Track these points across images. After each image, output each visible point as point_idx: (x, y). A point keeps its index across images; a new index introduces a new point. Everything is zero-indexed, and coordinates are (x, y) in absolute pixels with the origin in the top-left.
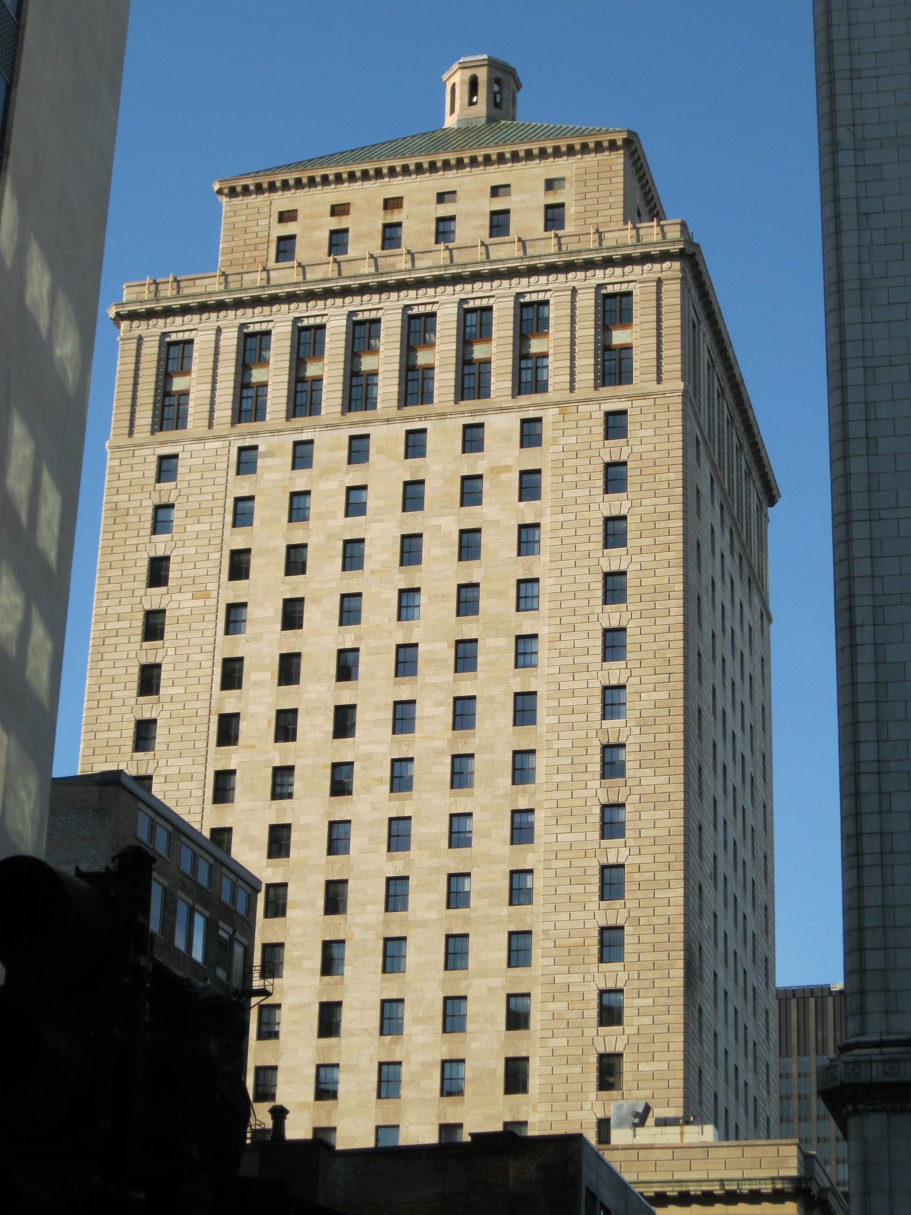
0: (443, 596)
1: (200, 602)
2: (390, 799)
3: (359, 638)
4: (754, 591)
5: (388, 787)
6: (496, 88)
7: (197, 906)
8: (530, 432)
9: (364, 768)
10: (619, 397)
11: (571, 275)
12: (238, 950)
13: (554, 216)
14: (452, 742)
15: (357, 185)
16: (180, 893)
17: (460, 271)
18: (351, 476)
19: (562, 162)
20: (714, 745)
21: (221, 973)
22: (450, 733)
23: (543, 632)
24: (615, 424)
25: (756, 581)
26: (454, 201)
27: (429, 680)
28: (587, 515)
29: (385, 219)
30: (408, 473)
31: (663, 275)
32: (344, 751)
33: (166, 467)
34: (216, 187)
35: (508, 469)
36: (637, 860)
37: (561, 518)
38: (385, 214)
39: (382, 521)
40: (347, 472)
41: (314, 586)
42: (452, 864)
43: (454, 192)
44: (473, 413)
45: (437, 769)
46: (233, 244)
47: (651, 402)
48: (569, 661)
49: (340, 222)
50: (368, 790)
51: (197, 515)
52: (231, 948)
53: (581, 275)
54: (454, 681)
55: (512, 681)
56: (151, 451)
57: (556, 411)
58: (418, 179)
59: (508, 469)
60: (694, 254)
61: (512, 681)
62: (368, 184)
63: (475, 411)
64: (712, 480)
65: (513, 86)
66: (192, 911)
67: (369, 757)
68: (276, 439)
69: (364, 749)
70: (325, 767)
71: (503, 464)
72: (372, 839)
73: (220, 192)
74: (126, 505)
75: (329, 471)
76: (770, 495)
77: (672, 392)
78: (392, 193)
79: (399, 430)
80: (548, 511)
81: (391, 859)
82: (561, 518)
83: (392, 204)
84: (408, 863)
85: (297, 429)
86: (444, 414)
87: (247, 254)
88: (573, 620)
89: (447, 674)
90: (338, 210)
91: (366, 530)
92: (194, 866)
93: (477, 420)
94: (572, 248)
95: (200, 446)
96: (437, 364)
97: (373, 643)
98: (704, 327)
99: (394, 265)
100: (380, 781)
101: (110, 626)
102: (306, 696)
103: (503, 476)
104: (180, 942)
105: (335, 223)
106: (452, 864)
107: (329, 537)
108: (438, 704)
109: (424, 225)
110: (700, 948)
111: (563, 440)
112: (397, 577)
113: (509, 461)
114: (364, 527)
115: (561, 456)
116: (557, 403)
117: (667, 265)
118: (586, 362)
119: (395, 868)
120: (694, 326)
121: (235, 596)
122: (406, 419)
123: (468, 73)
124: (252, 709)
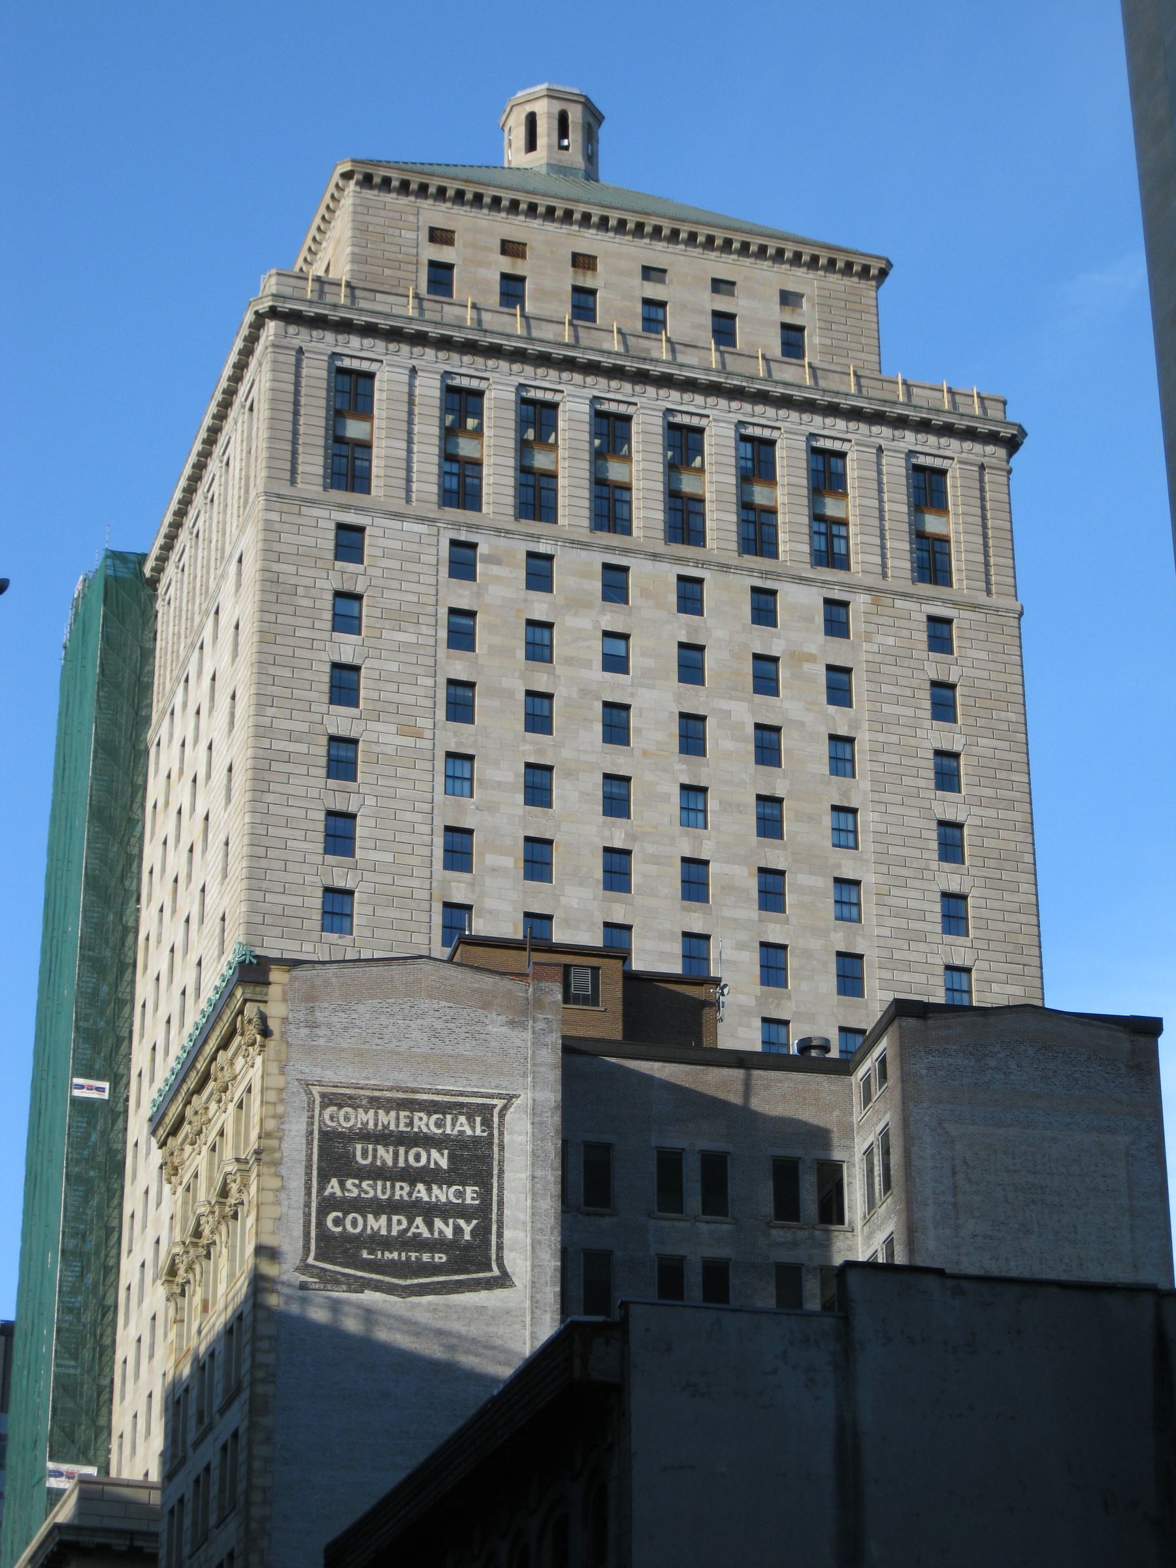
0: (739, 805)
1: (409, 741)
3: (633, 837)
8: (836, 619)
10: (944, 601)
11: (876, 429)
13: (792, 340)
15: (551, 227)
17: (744, 384)
18: (608, 617)
19: (799, 274)
22: (758, 989)
23: (869, 879)
24: (939, 634)
26: (663, 282)
27: (727, 913)
28: (912, 741)
29: (575, 279)
30: (684, 632)
31: (986, 461)
33: (349, 543)
34: (347, 167)
35: (811, 658)
37: (881, 737)
38: (575, 273)
39: (653, 687)
40: (602, 612)
41: (566, 753)
43: (664, 271)
44: (765, 574)
46: (367, 252)
47: (981, 617)
48: (903, 923)
49: (514, 265)
51: (399, 618)
54: (760, 921)
55: (833, 936)
56: (325, 514)
58: (617, 240)
59: (811, 658)
61: (833, 936)
63: (767, 573)
68: (502, 542)
71: (805, 650)
73: (347, 176)
74: (293, 580)
75: (576, 603)
77: (1008, 611)
79: (669, 573)
80: (866, 725)
82: (881, 737)
85: (532, 536)
86: (728, 567)
87: (387, 272)
88: (904, 872)
89: (752, 911)
91: (632, 695)
93: (768, 584)
94: (834, 387)
95: (396, 524)
96: (708, 496)
97: (651, 849)
99: (648, 350)
101: (277, 745)
102: (564, 900)
103: (807, 666)
105: (507, 265)
107: (584, 692)
108: (741, 946)
109: (628, 304)
111: (879, 639)
112: (679, 767)
113: (812, 648)
114: (630, 690)
115: (878, 658)
117: (990, 449)
118: (900, 547)
121: (459, 744)
122: (678, 560)
123: (557, 106)
124: (490, 903)
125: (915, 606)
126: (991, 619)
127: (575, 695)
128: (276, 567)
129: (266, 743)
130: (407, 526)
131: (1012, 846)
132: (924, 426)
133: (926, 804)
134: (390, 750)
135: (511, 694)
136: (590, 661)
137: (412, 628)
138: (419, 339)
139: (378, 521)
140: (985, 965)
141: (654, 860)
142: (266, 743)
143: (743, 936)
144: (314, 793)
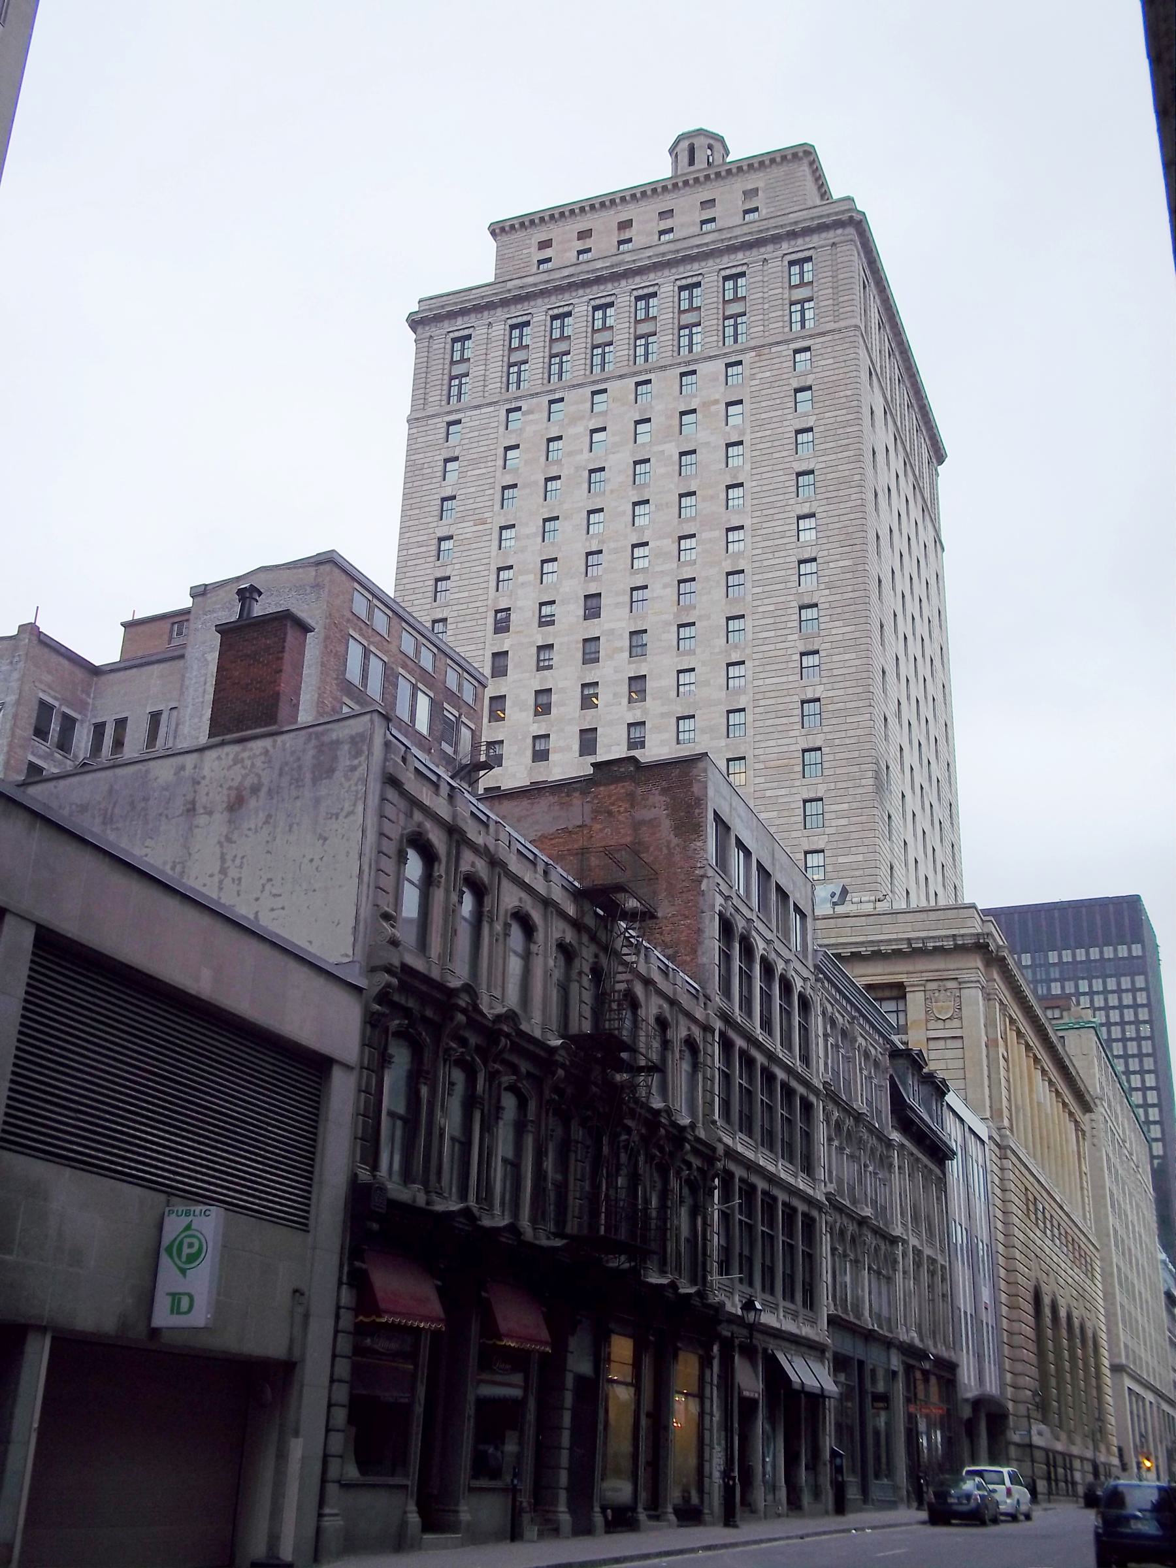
2: (629, 663)
3: (601, 542)
4: (927, 518)
5: (627, 654)
6: (709, 152)
7: (420, 685)
9: (608, 641)
12: (465, 734)
14: (677, 615)
16: (401, 670)
20: (895, 615)
21: (449, 750)
25: (930, 509)
27: (658, 569)
32: (593, 628)
35: (716, 402)
36: (830, 694)
40: (590, 419)
42: (679, 709)
45: (665, 636)
50: (611, 657)
51: (475, 463)
52: (458, 731)
53: (770, 248)
55: (724, 563)
56: (440, 420)
57: (753, 354)
59: (716, 402)
60: (861, 221)
62: (604, 213)
64: (885, 413)
65: (722, 151)
66: (415, 688)
67: (612, 631)
69: (606, 627)
70: (577, 642)
72: (615, 695)
75: (574, 420)
76: (938, 455)
78: (624, 217)
80: (748, 431)
81: (630, 709)
83: (625, 225)
84: (645, 712)
86: (665, 366)
90: (584, 235)
92: (417, 652)
95: (478, 412)
97: (612, 545)
98: (872, 290)
100: (621, 650)
103: (713, 408)
104: (402, 712)
106: (679, 709)
107: (577, 468)
108: (665, 586)
110: (888, 767)
113: (717, 396)
116: (753, 348)
119: (634, 716)
120: (864, 287)
124: (520, 604)
125: (785, 347)
126: (837, 337)
127: (572, 471)
128: (413, 458)
129: (405, 553)
130: (483, 411)
131: (847, 473)
132: (793, 235)
133: (788, 465)
134: (468, 536)
135: (536, 483)
136: (582, 450)
137: (482, 465)
138: (490, 306)
139: (468, 414)
140: (825, 553)
141: (615, 551)
142: (405, 553)
143: (667, 579)
144: (428, 571)
